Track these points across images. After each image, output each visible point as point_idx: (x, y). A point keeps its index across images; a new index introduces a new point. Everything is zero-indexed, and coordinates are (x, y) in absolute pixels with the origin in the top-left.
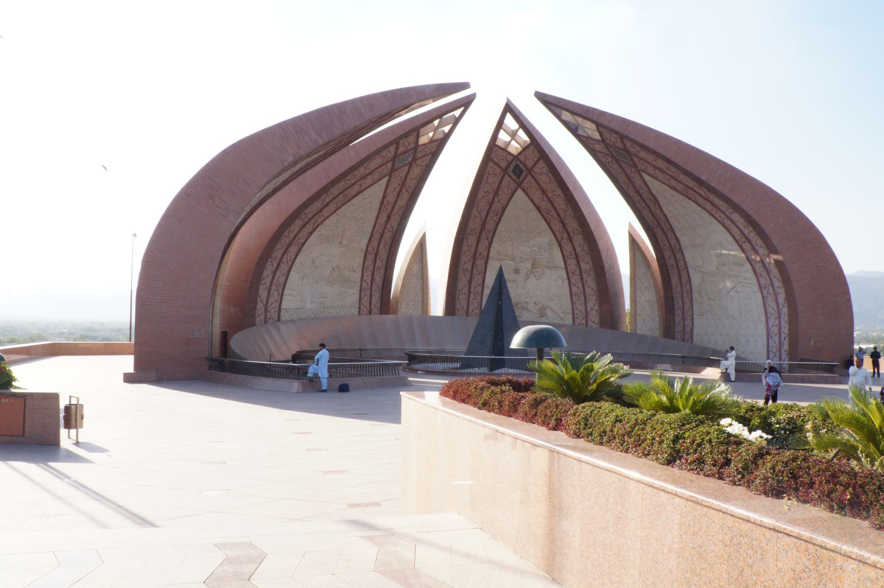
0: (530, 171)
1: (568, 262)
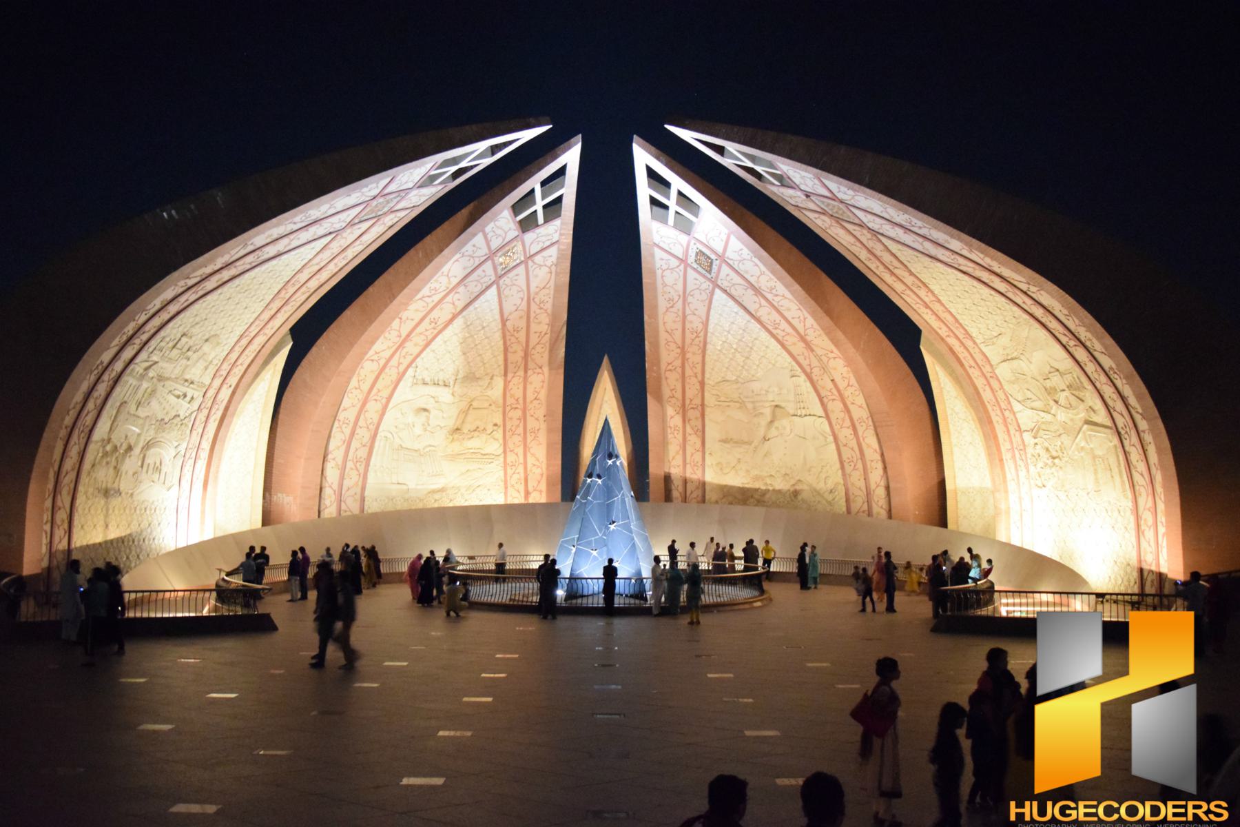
0: (722, 258)
1: (830, 406)
